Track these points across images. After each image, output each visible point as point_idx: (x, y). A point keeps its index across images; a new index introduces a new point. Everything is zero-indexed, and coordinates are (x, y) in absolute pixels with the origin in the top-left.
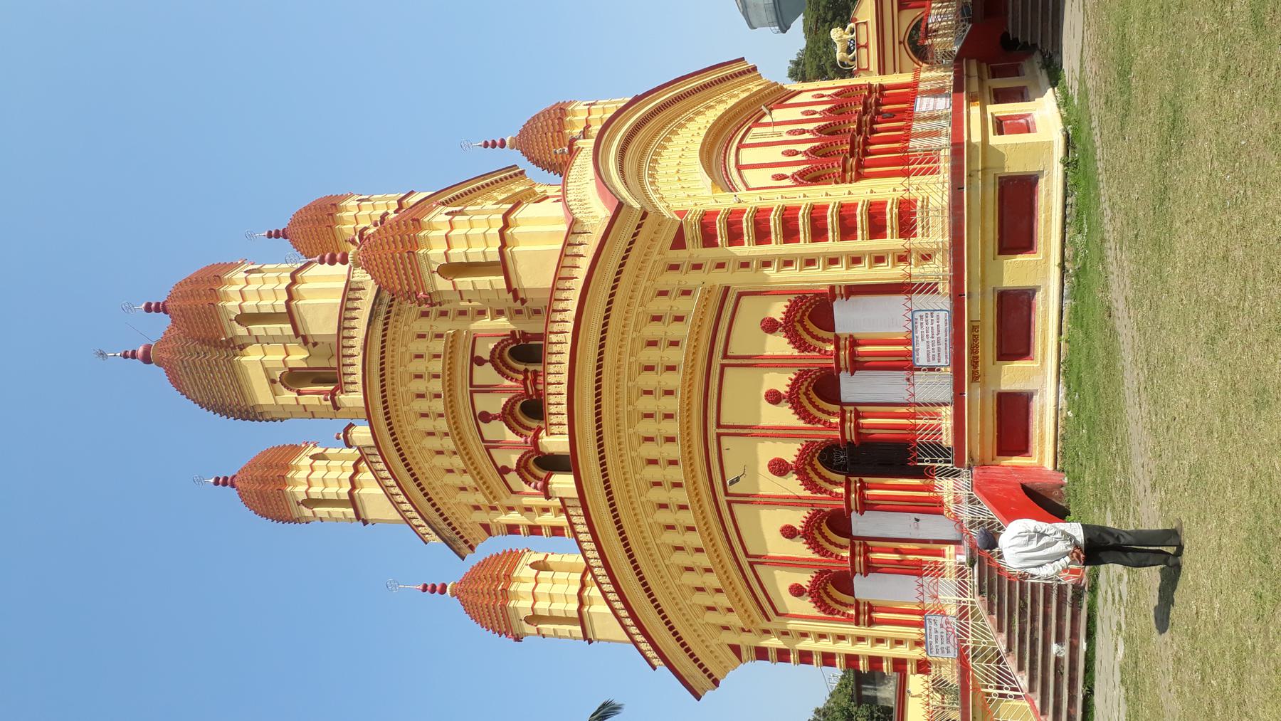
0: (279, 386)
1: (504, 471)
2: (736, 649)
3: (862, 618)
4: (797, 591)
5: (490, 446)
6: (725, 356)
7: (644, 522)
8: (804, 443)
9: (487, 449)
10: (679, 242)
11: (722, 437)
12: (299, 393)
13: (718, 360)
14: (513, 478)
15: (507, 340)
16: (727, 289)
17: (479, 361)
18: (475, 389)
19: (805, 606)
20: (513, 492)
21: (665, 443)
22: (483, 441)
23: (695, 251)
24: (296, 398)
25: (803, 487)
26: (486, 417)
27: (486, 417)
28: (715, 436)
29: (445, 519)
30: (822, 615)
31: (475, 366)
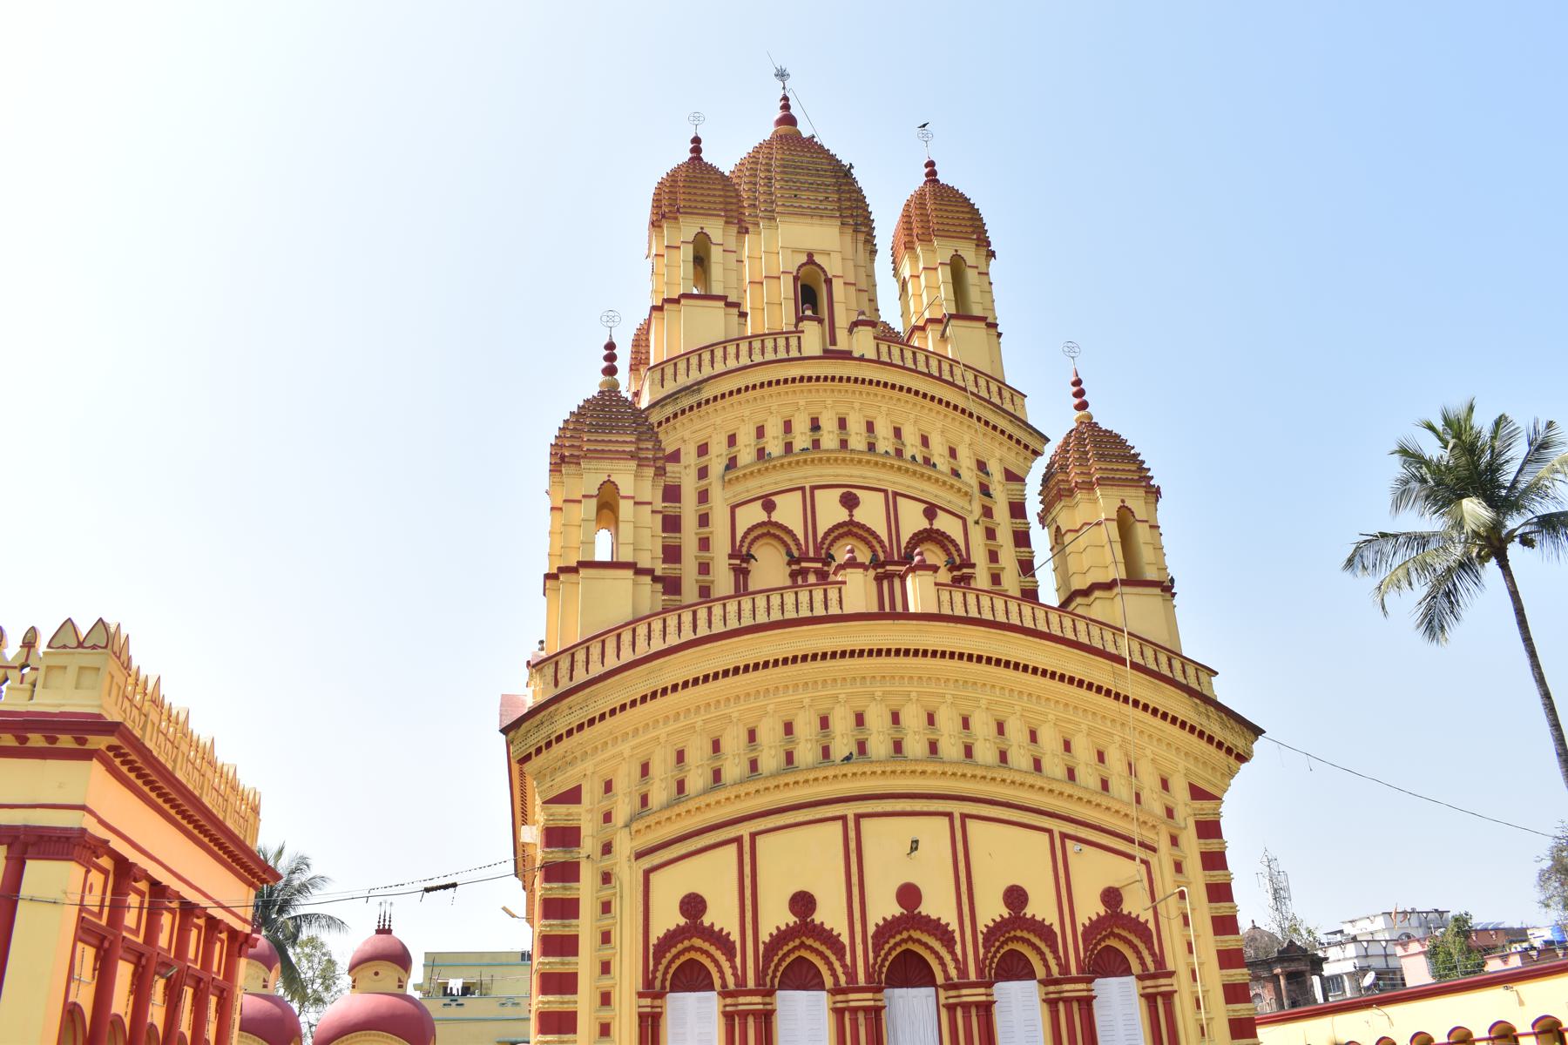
0: (804, 259)
1: (769, 506)
2: (572, 796)
3: (648, 1001)
4: (693, 905)
5: (809, 495)
6: (1064, 836)
7: (806, 697)
8: (950, 928)
9: (802, 489)
10: (1197, 793)
11: (947, 818)
12: (796, 279)
13: (1057, 826)
14: (752, 515)
15: (960, 555)
16: (1154, 850)
17: (931, 511)
18: (892, 499)
19: (668, 918)
20: (733, 509)
21: (928, 739)
22: (813, 488)
23: (1186, 812)
24: (791, 273)
25: (881, 923)
26: (850, 502)
27: (850, 502)
28: (948, 809)
29: (699, 405)
30: (653, 940)
31: (923, 506)
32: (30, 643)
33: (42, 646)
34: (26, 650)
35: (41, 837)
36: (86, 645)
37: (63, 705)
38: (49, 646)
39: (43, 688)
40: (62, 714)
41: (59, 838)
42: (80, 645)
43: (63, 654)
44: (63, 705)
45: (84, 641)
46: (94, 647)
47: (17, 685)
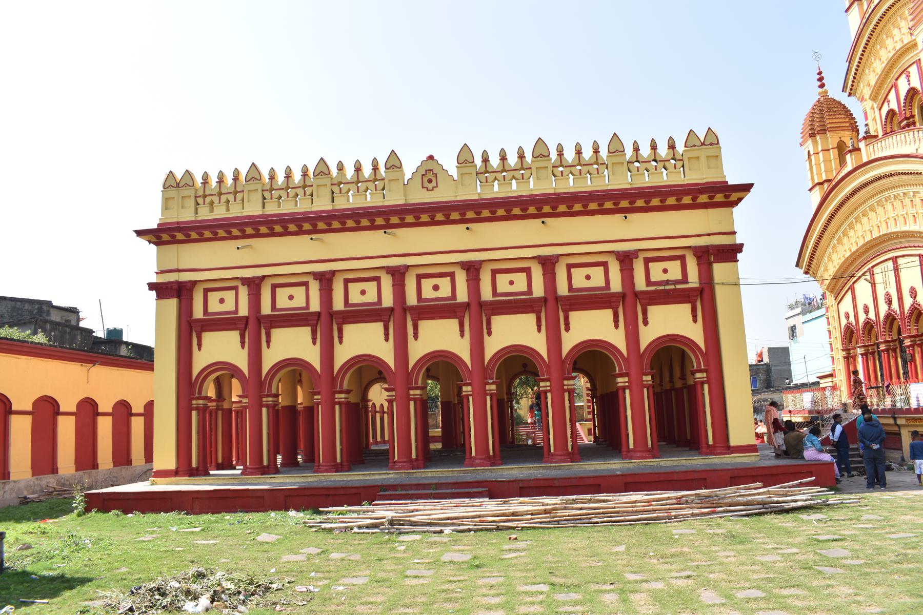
32: (672, 146)
33: (680, 148)
34: (672, 150)
35: (718, 250)
36: (706, 143)
37: (705, 178)
38: (685, 146)
39: (708, 168)
40: (707, 183)
41: (728, 250)
42: (703, 144)
43: (694, 150)
44: (705, 178)
45: (704, 141)
46: (711, 144)
47: (674, 170)
